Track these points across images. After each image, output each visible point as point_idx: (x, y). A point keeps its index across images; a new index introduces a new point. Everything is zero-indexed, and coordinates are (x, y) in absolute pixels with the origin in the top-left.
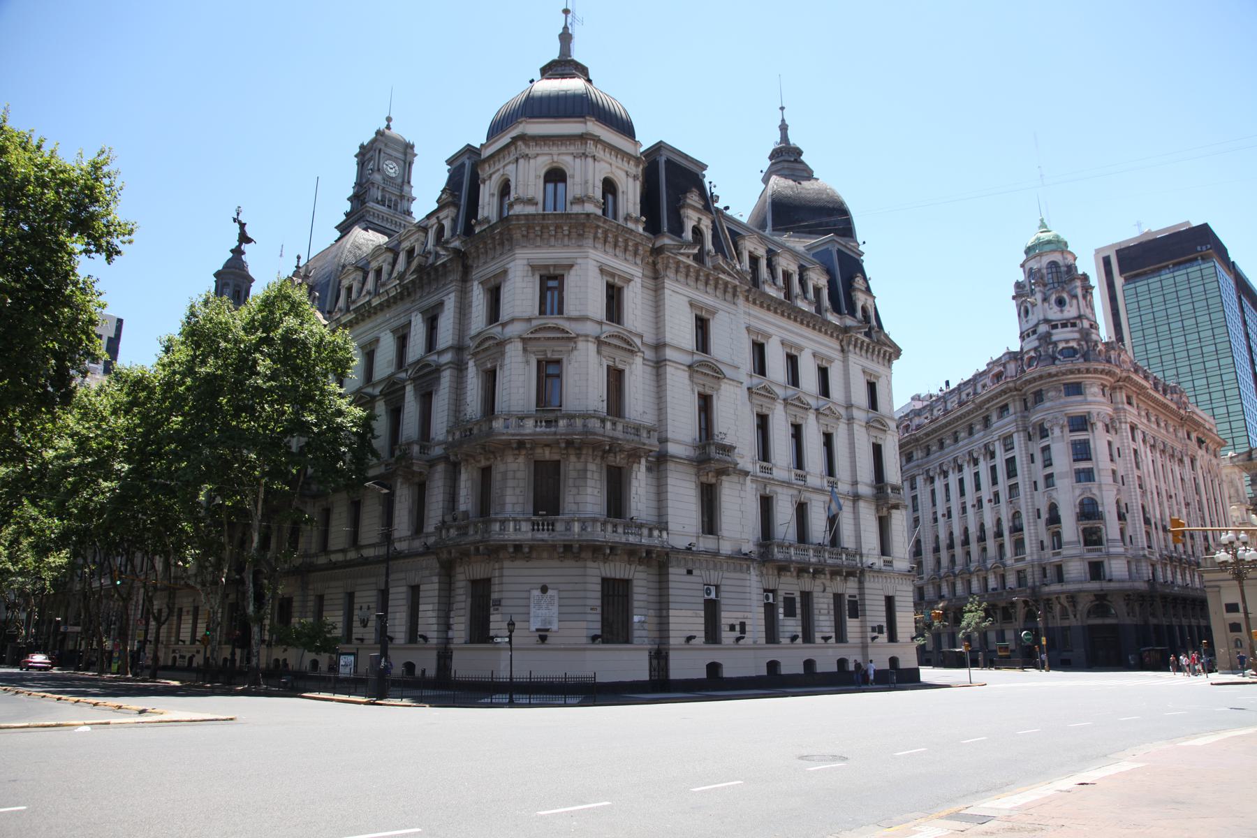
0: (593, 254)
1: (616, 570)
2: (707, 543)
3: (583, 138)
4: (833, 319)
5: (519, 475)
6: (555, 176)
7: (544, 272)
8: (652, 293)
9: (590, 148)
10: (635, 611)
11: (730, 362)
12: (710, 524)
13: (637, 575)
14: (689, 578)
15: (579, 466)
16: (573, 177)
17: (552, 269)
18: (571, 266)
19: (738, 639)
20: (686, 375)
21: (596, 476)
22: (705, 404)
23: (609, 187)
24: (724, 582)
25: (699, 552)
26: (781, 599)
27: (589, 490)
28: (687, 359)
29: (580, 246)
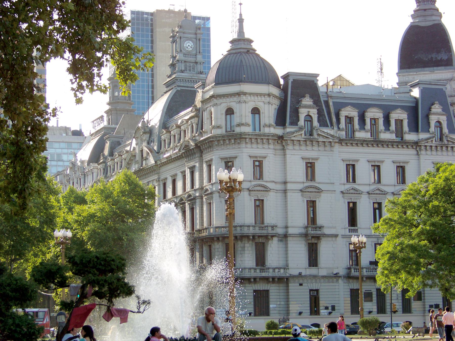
0: (245, 150)
1: (261, 286)
2: (313, 271)
3: (239, 94)
4: (410, 137)
5: (220, 250)
6: (230, 112)
7: (226, 161)
8: (283, 156)
9: (243, 98)
10: (271, 303)
12: (313, 261)
13: (272, 288)
14: (301, 287)
15: (242, 245)
16: (236, 113)
17: (228, 159)
18: (236, 157)
19: (330, 313)
20: (300, 194)
21: (250, 249)
22: (312, 205)
23: (256, 111)
24: (321, 287)
25: (305, 276)
27: (246, 255)
28: (301, 186)
29: (239, 148)
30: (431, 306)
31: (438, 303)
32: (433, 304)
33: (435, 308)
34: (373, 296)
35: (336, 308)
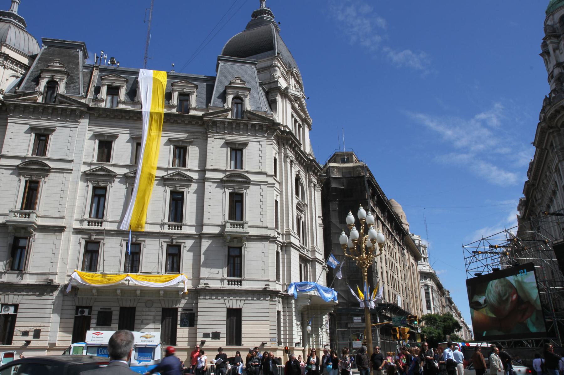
11: (66, 158)
26: (96, 313)
30: (206, 335)
31: (218, 331)
32: (210, 331)
33: (213, 338)
34: (113, 317)
35: (42, 334)
